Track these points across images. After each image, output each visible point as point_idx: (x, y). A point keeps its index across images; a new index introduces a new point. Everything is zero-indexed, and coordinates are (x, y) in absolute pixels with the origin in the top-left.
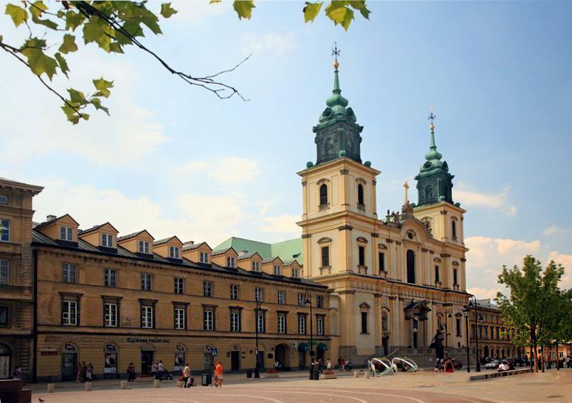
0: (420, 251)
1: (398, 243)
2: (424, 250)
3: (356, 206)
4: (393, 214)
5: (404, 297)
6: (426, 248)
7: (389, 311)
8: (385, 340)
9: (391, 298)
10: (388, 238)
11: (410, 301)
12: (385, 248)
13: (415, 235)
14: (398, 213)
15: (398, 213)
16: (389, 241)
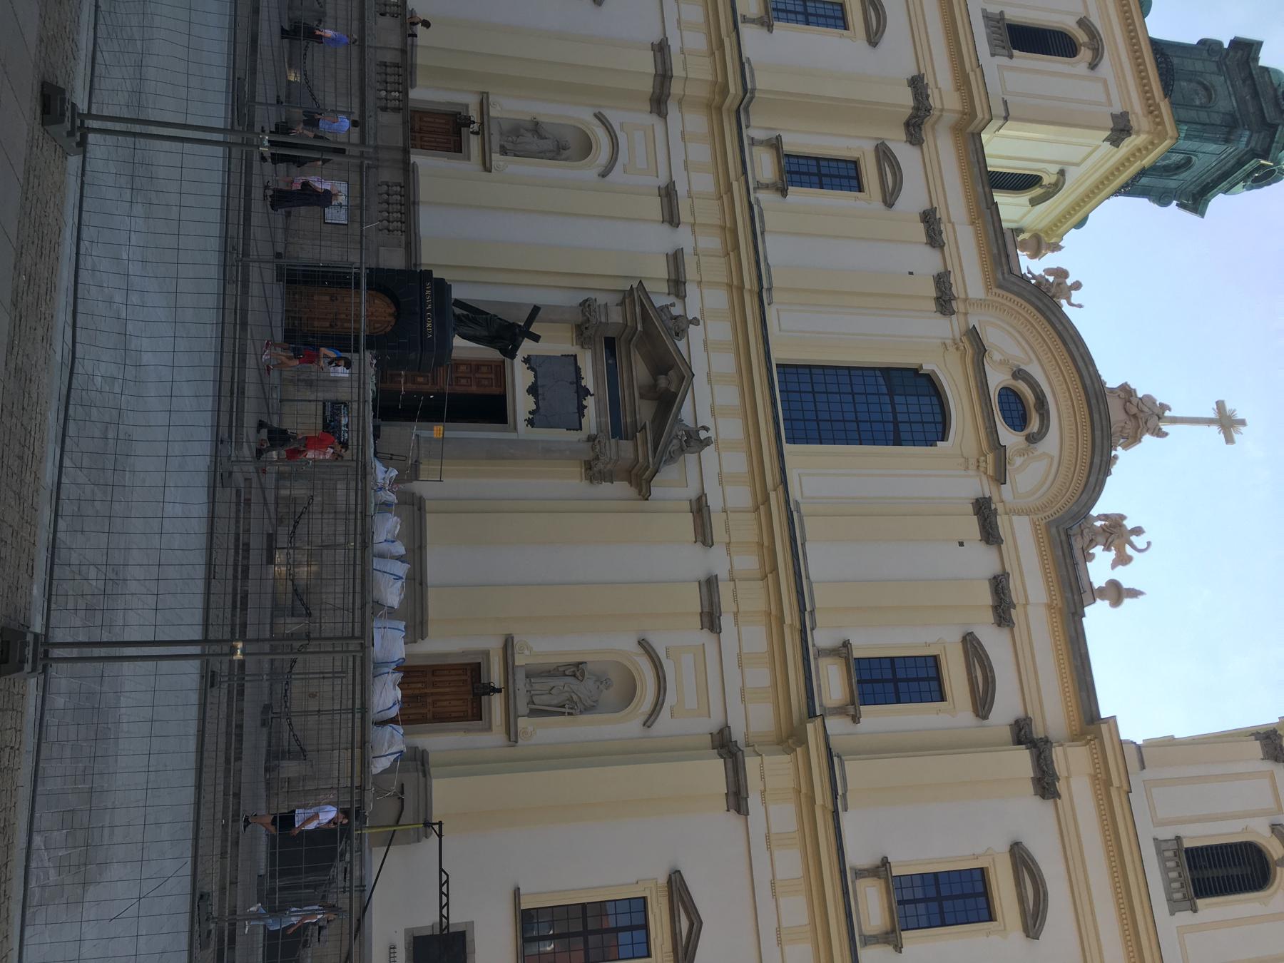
0: (975, 485)
1: (942, 281)
2: (984, 510)
3: (994, 9)
4: (1061, 274)
5: (691, 289)
6: (1002, 522)
7: (603, 175)
8: (449, 131)
9: (668, 194)
10: (939, 203)
11: (676, 311)
12: (889, 199)
13: (1032, 439)
14: (1077, 286)
15: (1077, 286)
16: (930, 219)
